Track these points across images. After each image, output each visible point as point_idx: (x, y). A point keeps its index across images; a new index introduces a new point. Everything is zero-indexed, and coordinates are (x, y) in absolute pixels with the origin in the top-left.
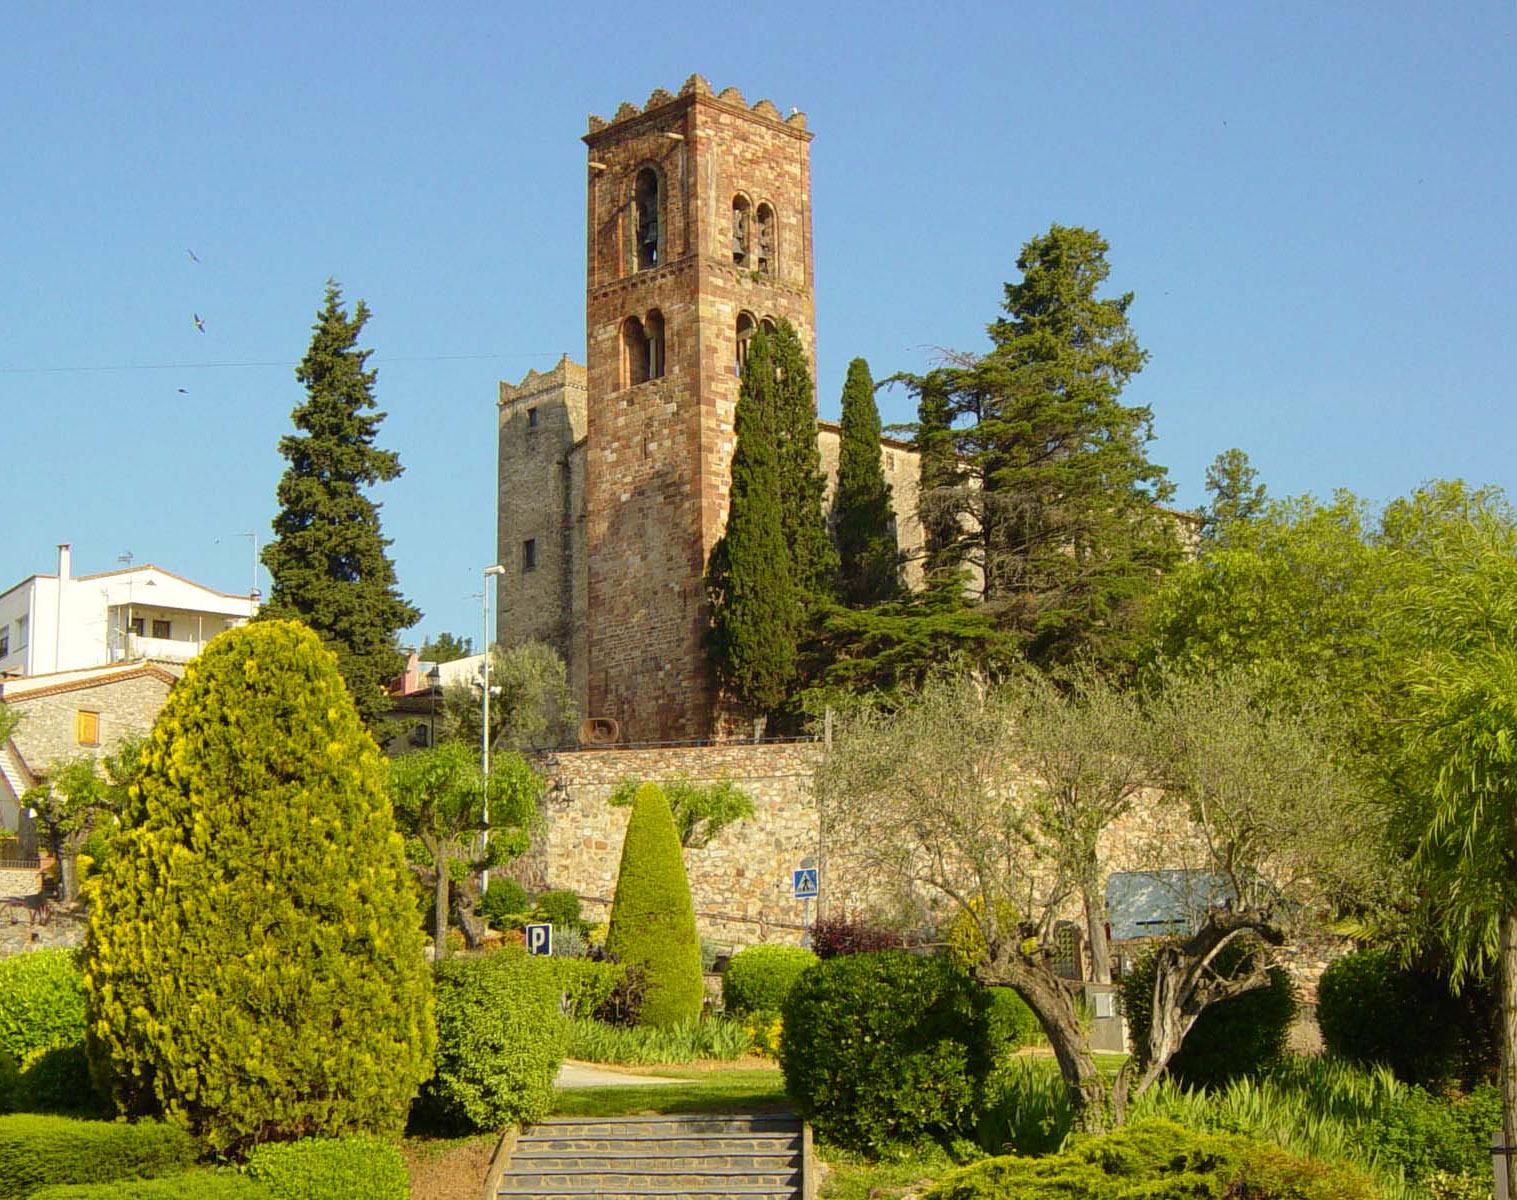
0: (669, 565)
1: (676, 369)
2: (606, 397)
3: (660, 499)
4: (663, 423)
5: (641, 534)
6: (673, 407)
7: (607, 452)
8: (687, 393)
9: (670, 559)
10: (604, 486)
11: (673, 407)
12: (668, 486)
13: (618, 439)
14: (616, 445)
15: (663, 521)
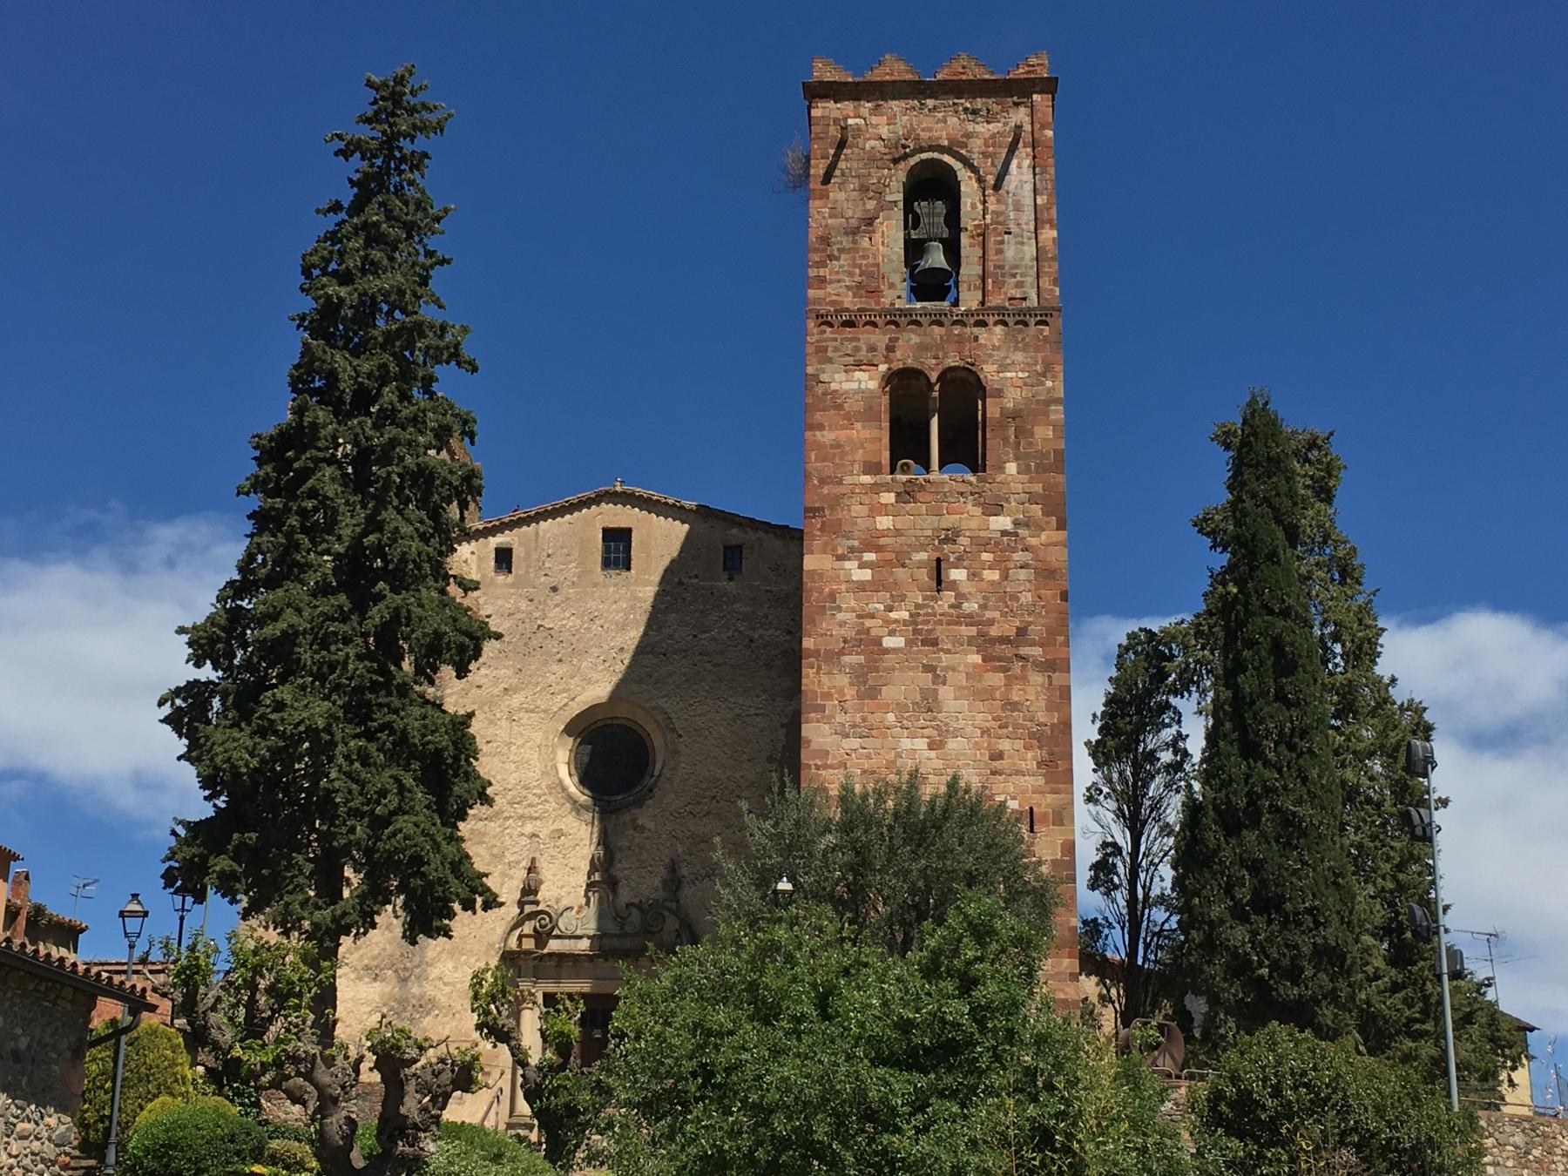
0: (997, 764)
1: (1012, 468)
2: (848, 480)
3: (977, 659)
4: (984, 544)
5: (929, 703)
6: (1003, 522)
7: (851, 565)
8: (1037, 510)
9: (997, 756)
10: (840, 616)
11: (1003, 522)
12: (995, 641)
13: (878, 549)
14: (870, 557)
15: (986, 695)
